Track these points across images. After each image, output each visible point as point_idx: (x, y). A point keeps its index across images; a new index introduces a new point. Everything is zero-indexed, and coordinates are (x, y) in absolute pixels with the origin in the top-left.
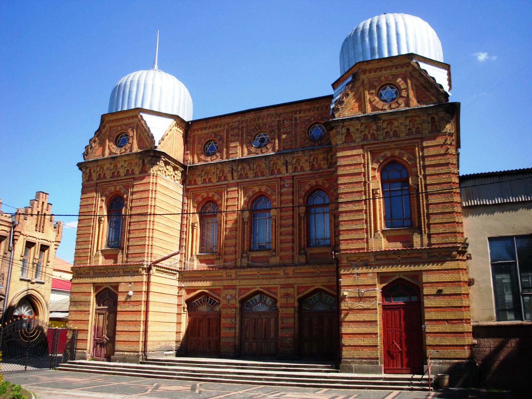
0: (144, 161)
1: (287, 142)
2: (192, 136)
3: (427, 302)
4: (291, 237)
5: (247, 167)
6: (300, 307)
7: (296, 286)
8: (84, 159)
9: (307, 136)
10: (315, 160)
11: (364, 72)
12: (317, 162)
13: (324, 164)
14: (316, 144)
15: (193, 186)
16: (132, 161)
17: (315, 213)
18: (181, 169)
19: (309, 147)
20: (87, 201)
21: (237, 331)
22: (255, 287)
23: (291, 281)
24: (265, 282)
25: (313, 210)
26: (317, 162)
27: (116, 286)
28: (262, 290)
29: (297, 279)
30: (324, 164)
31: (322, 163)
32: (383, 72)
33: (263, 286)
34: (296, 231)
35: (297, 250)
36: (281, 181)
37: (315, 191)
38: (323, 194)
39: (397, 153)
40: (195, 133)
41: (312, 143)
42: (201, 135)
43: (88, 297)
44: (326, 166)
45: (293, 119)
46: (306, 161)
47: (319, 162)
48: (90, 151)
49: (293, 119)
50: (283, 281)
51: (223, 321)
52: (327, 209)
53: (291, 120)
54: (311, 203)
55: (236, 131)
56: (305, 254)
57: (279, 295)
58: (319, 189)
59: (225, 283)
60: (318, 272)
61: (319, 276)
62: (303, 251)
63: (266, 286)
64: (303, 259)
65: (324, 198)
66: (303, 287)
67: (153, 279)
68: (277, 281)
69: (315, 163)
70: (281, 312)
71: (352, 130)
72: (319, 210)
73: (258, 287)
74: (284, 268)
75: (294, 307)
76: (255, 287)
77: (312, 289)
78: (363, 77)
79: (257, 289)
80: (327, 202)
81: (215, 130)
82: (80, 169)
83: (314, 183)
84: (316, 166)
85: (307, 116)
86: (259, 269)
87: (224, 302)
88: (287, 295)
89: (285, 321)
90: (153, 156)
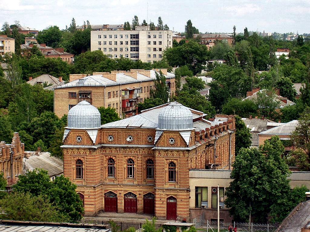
3: (178, 203)
4: (141, 176)
5: (125, 150)
6: (144, 198)
9: (146, 140)
11: (165, 133)
15: (104, 153)
20: (67, 161)
21: (123, 204)
23: (141, 190)
24: (132, 189)
27: (83, 192)
32: (171, 134)
34: (143, 175)
39: (173, 161)
50: (138, 189)
51: (118, 201)
59: (118, 189)
61: (150, 189)
64: (145, 183)
68: (136, 189)
71: (160, 152)
75: (142, 198)
78: (164, 134)
87: (118, 195)
88: (140, 194)
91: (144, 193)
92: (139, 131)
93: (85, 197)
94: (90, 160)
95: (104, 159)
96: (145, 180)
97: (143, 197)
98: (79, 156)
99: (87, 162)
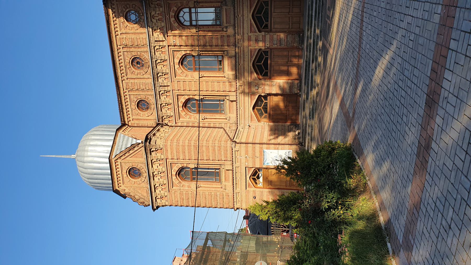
0: (153, 151)
1: (140, 42)
2: (133, 122)
7: (250, 34)
8: (149, 205)
10: (155, 18)
12: (157, 17)
13: (159, 11)
14: (143, 17)
16: (153, 161)
17: (196, 20)
18: (159, 127)
19: (145, 23)
22: (249, 67)
24: (246, 59)
25: (194, 23)
26: (157, 17)
28: (252, 62)
29: (245, 32)
30: (159, 11)
31: (157, 13)
33: (250, 60)
35: (224, 34)
36: (170, 46)
37: (180, 21)
38: (181, 14)
40: (131, 119)
41: (142, 21)
42: (132, 115)
43: (257, 192)
44: (161, 9)
45: (121, 37)
46: (155, 24)
47: (157, 15)
48: (142, 200)
49: (121, 37)
52: (193, 10)
53: (123, 38)
54: (188, 23)
55: (130, 85)
56: (226, 27)
57: (257, 47)
58: (178, 17)
60: (240, 16)
61: (243, 15)
62: (225, 30)
63: (249, 58)
65: (185, 13)
66: (251, 28)
67: (243, 141)
69: (157, 18)
70: (269, 46)
72: (194, 18)
73: (250, 65)
74: (237, 43)
76: (249, 67)
77: (252, 21)
79: (252, 65)
80: (187, 10)
81: (129, 103)
82: (158, 207)
83: (172, 19)
84: (160, 17)
85: (120, 25)
86: (237, 63)
89: (275, 42)
90: (150, 143)
91: (253, 28)
92: (119, 44)
93: (258, 166)
94: (175, 152)
95: (188, 120)
96: (225, 30)
97: (263, 33)
98: (170, 175)
99: (181, 158)
